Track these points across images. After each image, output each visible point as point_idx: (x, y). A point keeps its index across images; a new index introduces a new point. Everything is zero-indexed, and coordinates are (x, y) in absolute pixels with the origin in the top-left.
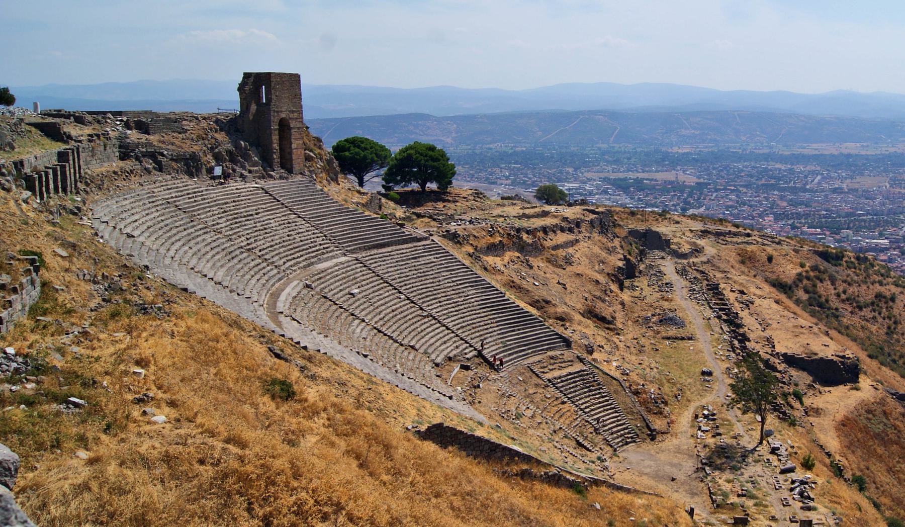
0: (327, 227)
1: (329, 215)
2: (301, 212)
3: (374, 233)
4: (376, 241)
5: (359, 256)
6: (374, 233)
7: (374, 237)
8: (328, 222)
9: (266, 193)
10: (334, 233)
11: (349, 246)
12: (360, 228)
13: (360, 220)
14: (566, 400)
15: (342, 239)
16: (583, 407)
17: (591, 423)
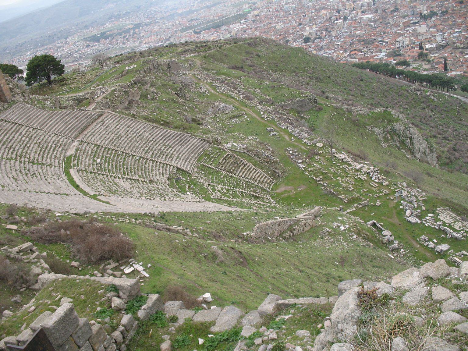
0: (52, 128)
1: (47, 120)
2: (32, 125)
3: (77, 121)
4: (81, 125)
5: (80, 138)
6: (77, 121)
7: (79, 123)
8: (51, 125)
9: (6, 121)
10: (59, 130)
11: (72, 135)
12: (69, 121)
13: (65, 116)
14: (231, 175)
15: (65, 132)
16: (240, 175)
17: (249, 182)
